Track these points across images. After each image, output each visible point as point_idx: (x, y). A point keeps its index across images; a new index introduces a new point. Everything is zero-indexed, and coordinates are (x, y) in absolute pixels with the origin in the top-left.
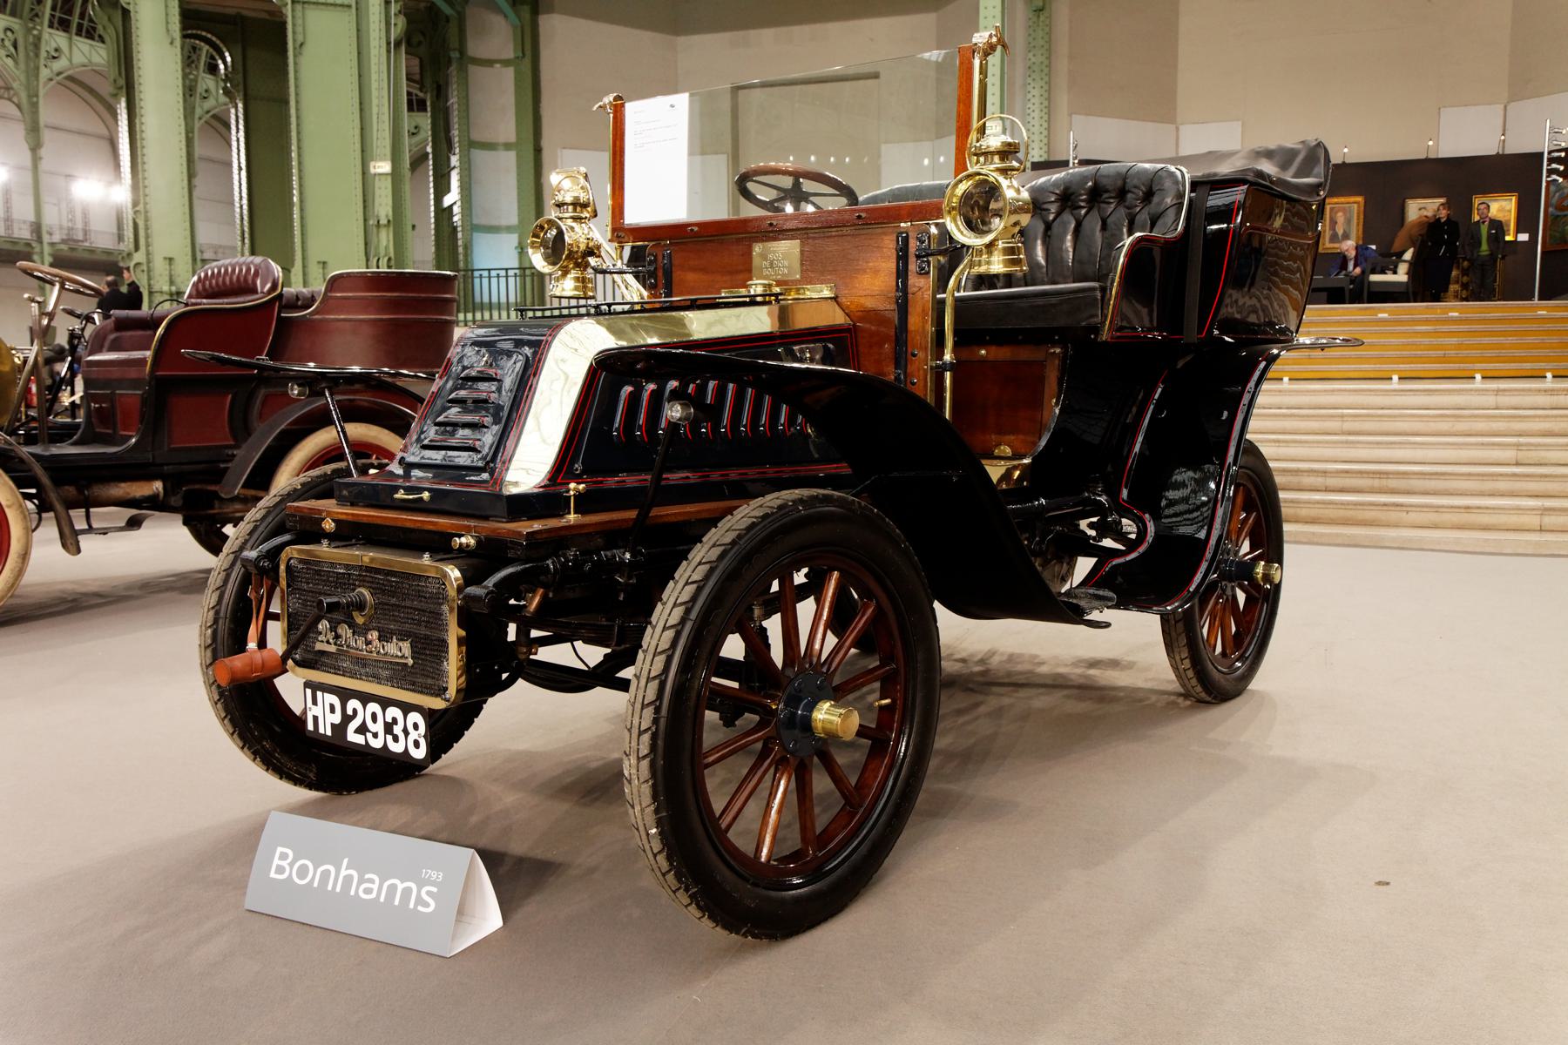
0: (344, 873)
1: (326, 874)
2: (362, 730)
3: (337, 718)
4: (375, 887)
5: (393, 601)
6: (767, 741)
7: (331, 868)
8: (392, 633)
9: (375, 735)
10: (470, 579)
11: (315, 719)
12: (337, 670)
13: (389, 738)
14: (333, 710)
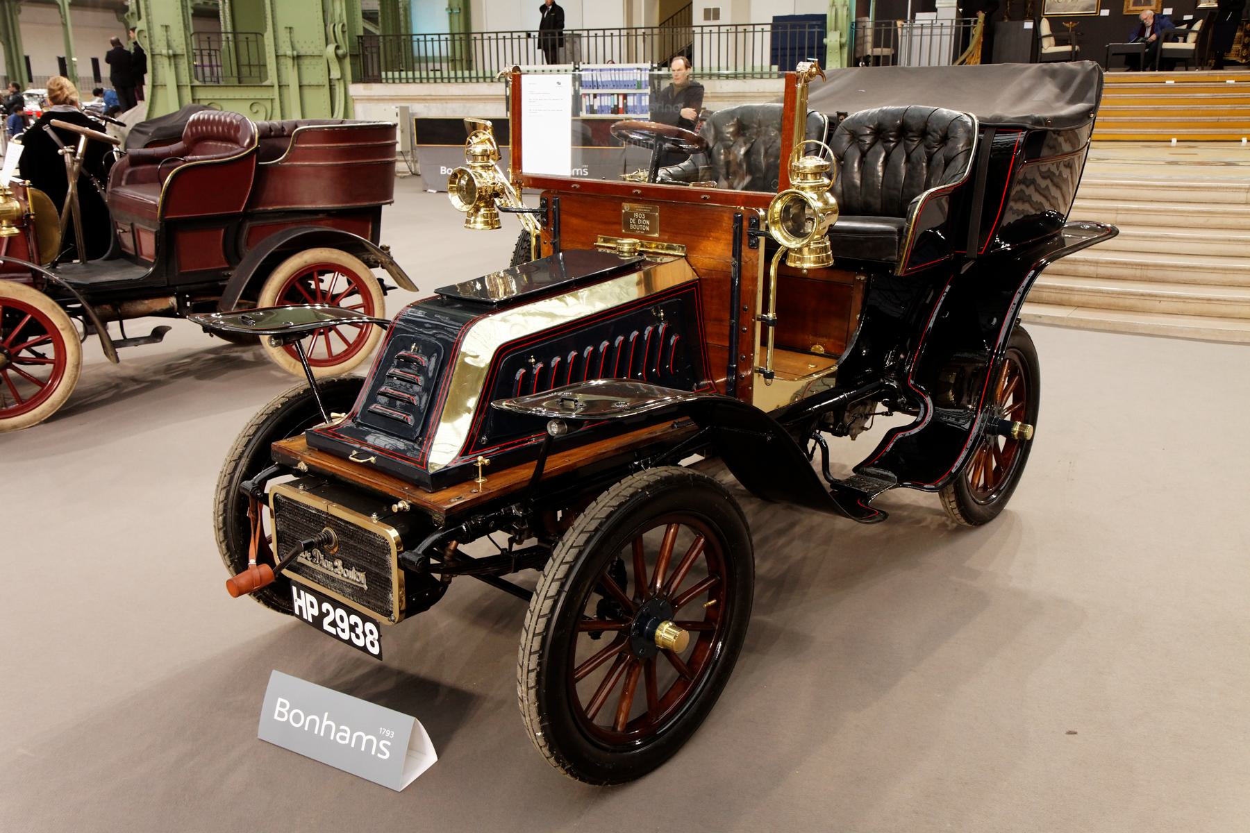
0: (325, 723)
1: (313, 722)
2: (333, 624)
3: (316, 612)
4: (348, 736)
5: (351, 542)
6: (621, 653)
8: (352, 565)
9: (343, 631)
10: (407, 542)
11: (300, 608)
12: (314, 579)
13: (353, 635)
14: (312, 605)
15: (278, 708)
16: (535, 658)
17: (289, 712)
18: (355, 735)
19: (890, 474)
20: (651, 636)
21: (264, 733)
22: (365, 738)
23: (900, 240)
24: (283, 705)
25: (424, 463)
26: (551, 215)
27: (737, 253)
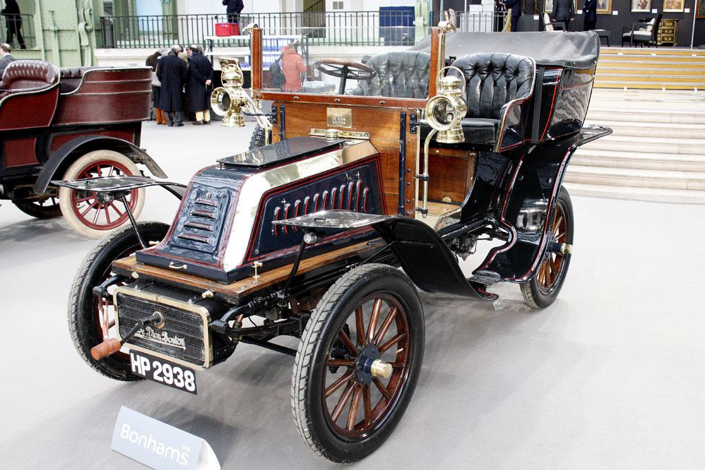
0: (150, 440)
2: (161, 375)
3: (148, 368)
5: (174, 320)
6: (349, 381)
7: (145, 437)
8: (175, 334)
9: (168, 378)
10: (215, 315)
11: (136, 367)
12: (146, 346)
13: (176, 380)
14: (145, 364)
15: (123, 430)
16: (303, 381)
17: (129, 432)
18: (167, 449)
19: (496, 274)
20: (368, 370)
21: (115, 445)
22: (173, 451)
23: (496, 130)
24: (126, 428)
25: (221, 266)
26: (279, 117)
27: (403, 137)
